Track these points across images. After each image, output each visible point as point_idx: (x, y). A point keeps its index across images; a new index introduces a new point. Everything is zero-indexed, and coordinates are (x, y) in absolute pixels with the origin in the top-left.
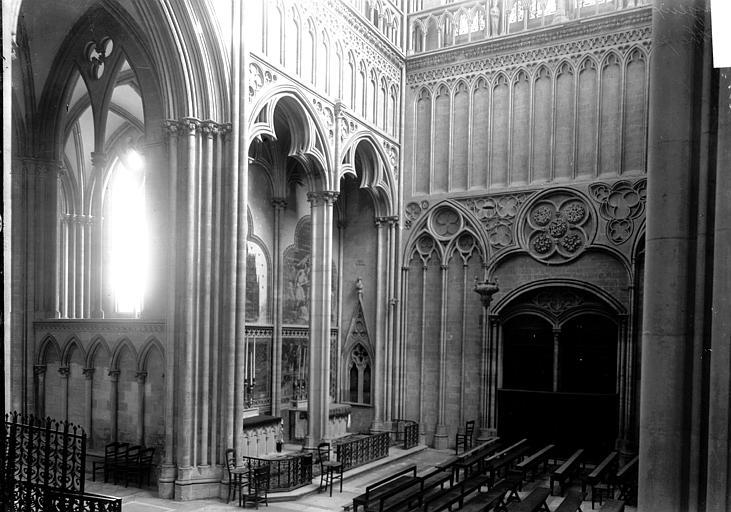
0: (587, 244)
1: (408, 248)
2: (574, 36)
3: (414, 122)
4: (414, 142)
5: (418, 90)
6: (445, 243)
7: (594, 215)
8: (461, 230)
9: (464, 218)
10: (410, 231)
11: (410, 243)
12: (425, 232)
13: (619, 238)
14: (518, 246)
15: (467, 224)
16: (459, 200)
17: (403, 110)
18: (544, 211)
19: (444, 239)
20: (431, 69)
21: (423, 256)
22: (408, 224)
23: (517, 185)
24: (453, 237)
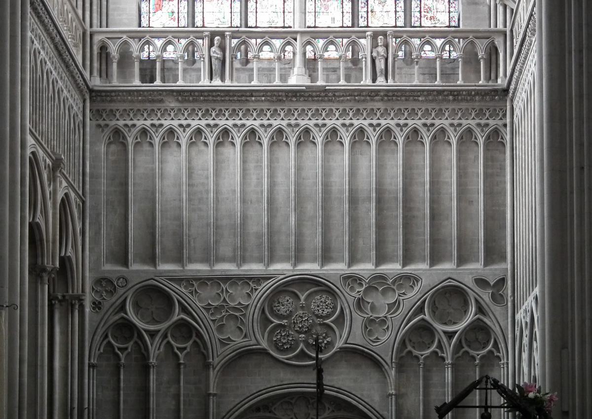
0: (339, 344)
1: (98, 338)
2: (318, 101)
3: (103, 171)
4: (103, 198)
5: (107, 131)
6: (152, 334)
7: (348, 310)
8: (175, 318)
9: (179, 302)
10: (100, 316)
11: (100, 332)
12: (123, 318)
13: (377, 338)
14: (253, 342)
15: (184, 309)
16: (170, 280)
17: (88, 154)
18: (286, 304)
19: (152, 328)
20: (127, 106)
21: (119, 349)
22: (97, 305)
23: (254, 268)
24: (163, 326)
